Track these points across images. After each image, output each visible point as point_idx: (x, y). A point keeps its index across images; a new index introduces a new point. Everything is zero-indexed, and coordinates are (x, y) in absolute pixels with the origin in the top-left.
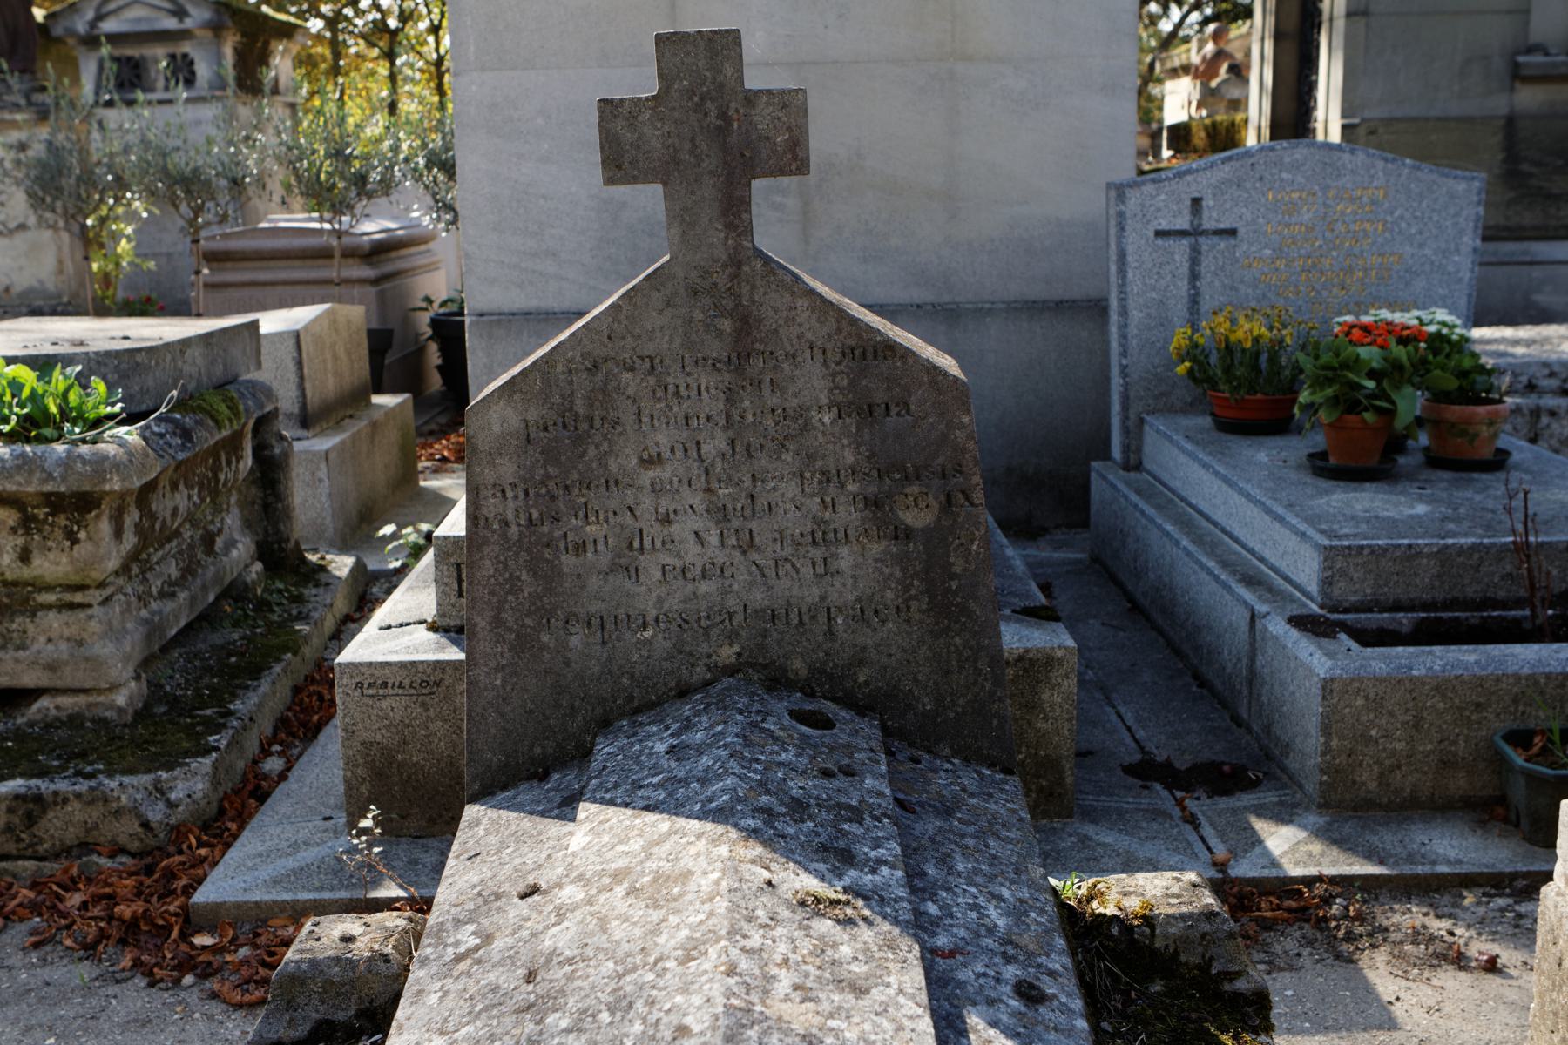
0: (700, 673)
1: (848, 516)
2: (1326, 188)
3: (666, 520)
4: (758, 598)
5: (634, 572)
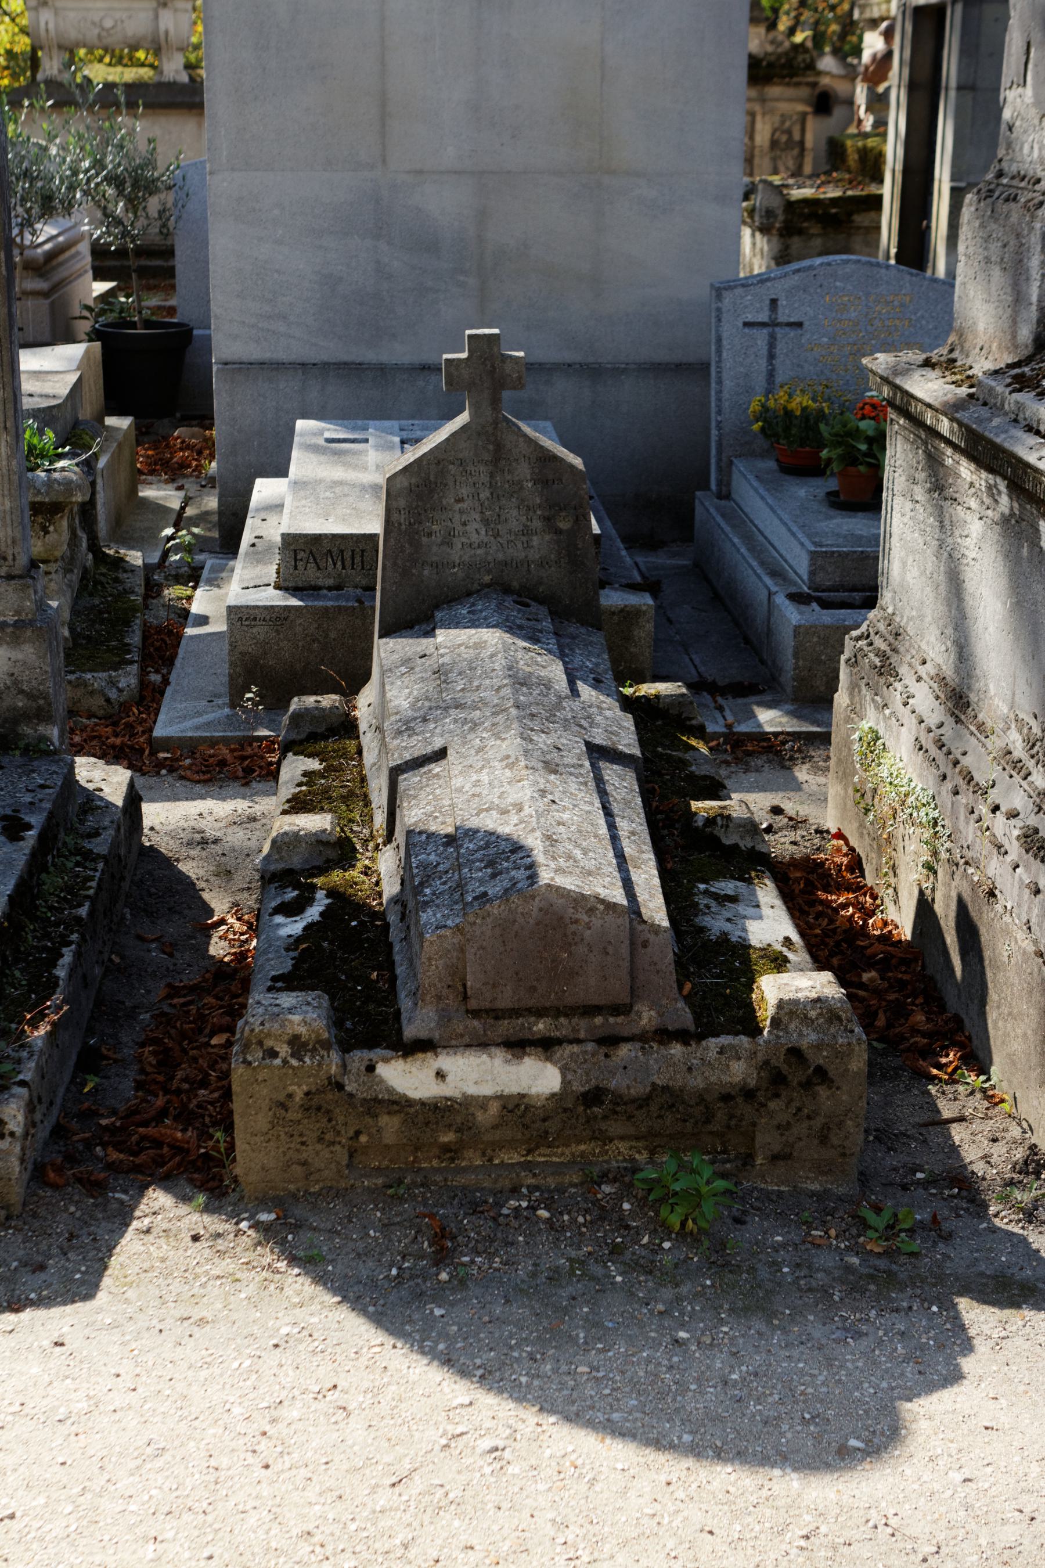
0: (476, 586)
1: (537, 524)
2: (868, 294)
3: (464, 524)
4: (500, 556)
5: (450, 545)
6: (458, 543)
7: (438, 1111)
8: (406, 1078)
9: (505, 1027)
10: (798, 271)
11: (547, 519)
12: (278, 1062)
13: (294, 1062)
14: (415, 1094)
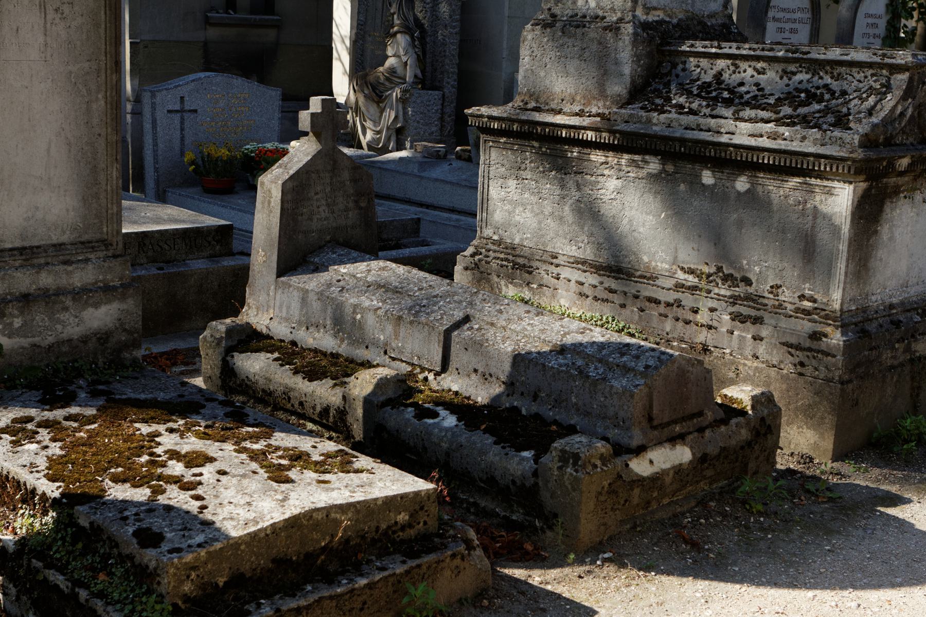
0: (323, 243)
1: (351, 205)
2: (228, 94)
3: (318, 207)
4: (334, 225)
5: (311, 220)
6: (315, 218)
7: (656, 480)
8: (641, 467)
9: (666, 432)
10: (193, 80)
11: (356, 202)
12: (599, 469)
13: (605, 468)
14: (645, 474)
